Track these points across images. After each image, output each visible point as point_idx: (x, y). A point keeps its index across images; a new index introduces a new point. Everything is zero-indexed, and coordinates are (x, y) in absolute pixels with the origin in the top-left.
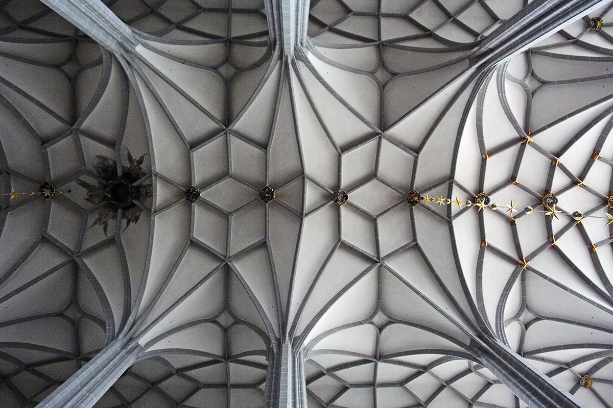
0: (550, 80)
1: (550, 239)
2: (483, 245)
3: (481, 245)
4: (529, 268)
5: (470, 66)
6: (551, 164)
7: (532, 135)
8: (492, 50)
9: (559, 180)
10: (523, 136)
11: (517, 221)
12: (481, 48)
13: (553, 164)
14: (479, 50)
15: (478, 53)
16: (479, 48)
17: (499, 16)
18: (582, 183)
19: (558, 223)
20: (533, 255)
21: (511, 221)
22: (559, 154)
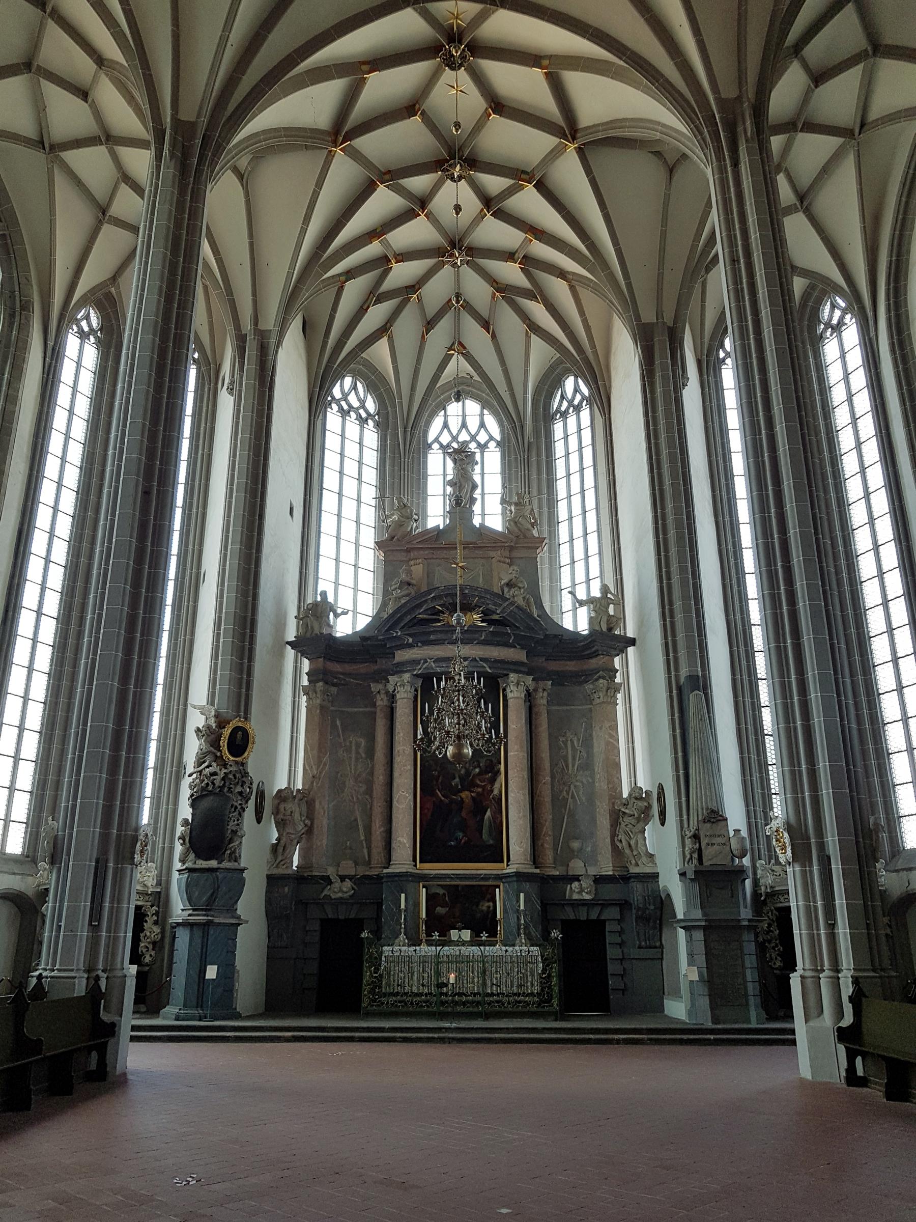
0: (673, 183)
1: (387, 177)
2: (365, 68)
3: (364, 63)
4: (330, 156)
5: (719, 100)
6: (524, 172)
7: (580, 151)
8: (736, 164)
9: (494, 183)
10: (578, 135)
11: (418, 118)
12: (747, 141)
13: (523, 176)
14: (745, 133)
15: (740, 129)
16: (749, 134)
17: (821, 88)
18: (488, 215)
19: (419, 183)
20: (355, 155)
21: (414, 105)
22: (542, 187)
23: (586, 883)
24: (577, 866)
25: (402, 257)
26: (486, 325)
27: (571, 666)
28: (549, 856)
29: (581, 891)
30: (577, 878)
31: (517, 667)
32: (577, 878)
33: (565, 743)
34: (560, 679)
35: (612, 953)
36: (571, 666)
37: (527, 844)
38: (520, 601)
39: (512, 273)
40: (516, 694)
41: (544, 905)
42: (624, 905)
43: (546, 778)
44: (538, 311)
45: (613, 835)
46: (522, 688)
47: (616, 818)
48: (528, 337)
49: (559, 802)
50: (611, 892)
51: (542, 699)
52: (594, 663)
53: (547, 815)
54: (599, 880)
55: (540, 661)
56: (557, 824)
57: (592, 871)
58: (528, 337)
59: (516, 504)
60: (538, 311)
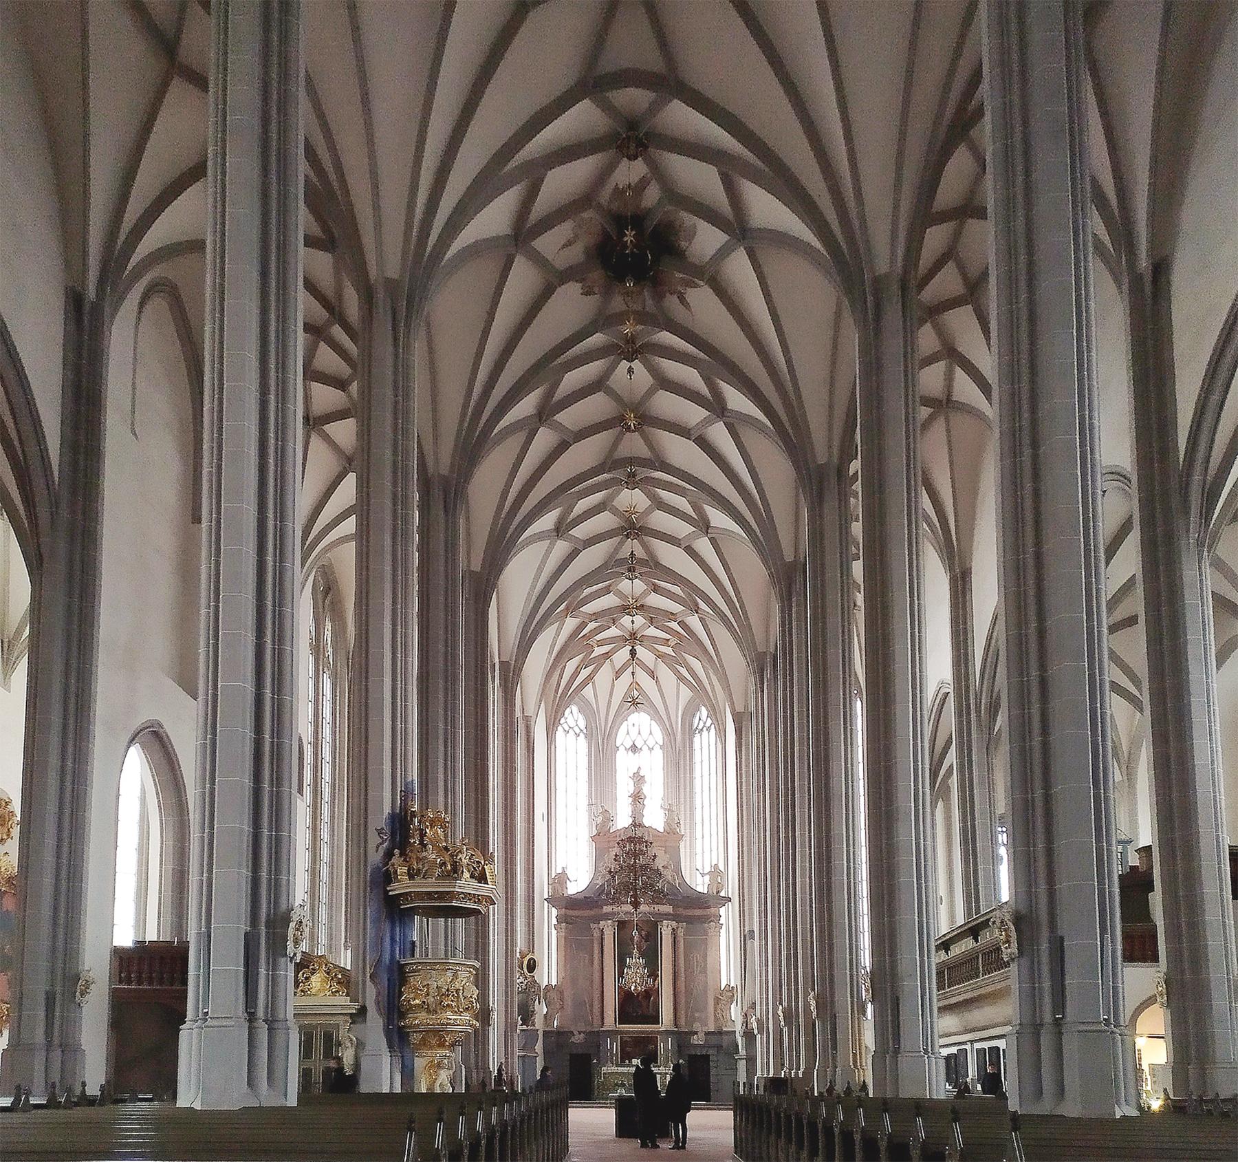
1: (594, 617)
23: (701, 1035)
24: (697, 1027)
25: (601, 643)
26: (652, 674)
27: (698, 912)
28: (682, 1021)
29: (698, 1040)
30: (696, 1033)
31: (667, 916)
32: (696, 1033)
33: (693, 957)
34: (690, 920)
35: (712, 1072)
36: (698, 912)
37: (671, 1016)
38: (670, 878)
39: (669, 651)
40: (666, 932)
41: (679, 1046)
42: (719, 1047)
43: (682, 978)
44: (684, 671)
45: (715, 1010)
46: (670, 928)
47: (717, 1001)
48: (678, 686)
49: (689, 992)
50: (714, 1040)
51: (681, 933)
52: (713, 910)
53: (682, 1000)
54: (707, 1034)
55: (681, 911)
56: (687, 1003)
57: (706, 1029)
58: (678, 686)
59: (669, 810)
60: (684, 671)
